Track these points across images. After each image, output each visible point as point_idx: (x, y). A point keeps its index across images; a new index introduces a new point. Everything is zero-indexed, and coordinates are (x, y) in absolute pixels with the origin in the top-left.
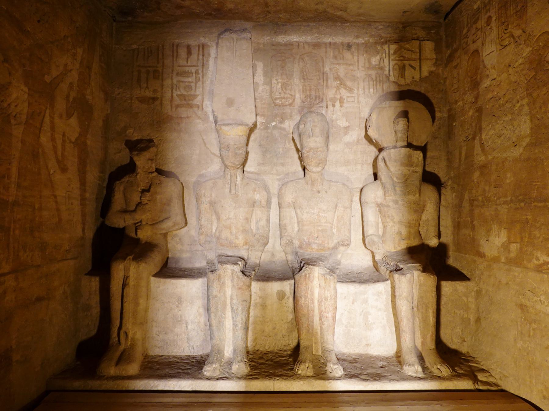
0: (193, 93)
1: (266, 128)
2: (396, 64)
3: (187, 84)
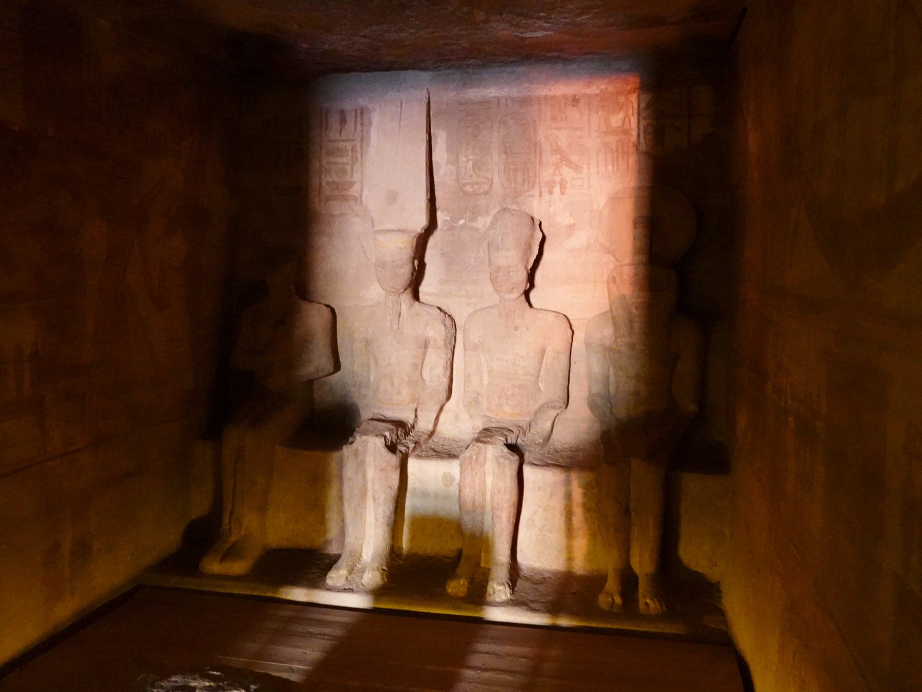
0: (348, 178)
1: (451, 228)
2: (648, 125)
3: (340, 166)
